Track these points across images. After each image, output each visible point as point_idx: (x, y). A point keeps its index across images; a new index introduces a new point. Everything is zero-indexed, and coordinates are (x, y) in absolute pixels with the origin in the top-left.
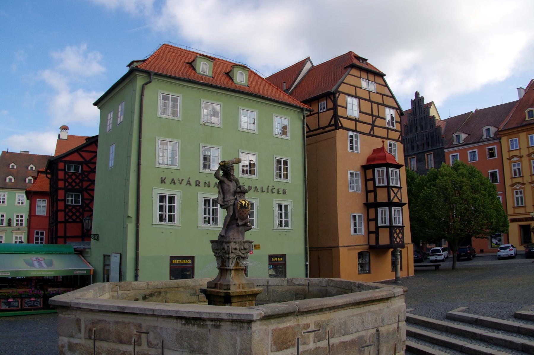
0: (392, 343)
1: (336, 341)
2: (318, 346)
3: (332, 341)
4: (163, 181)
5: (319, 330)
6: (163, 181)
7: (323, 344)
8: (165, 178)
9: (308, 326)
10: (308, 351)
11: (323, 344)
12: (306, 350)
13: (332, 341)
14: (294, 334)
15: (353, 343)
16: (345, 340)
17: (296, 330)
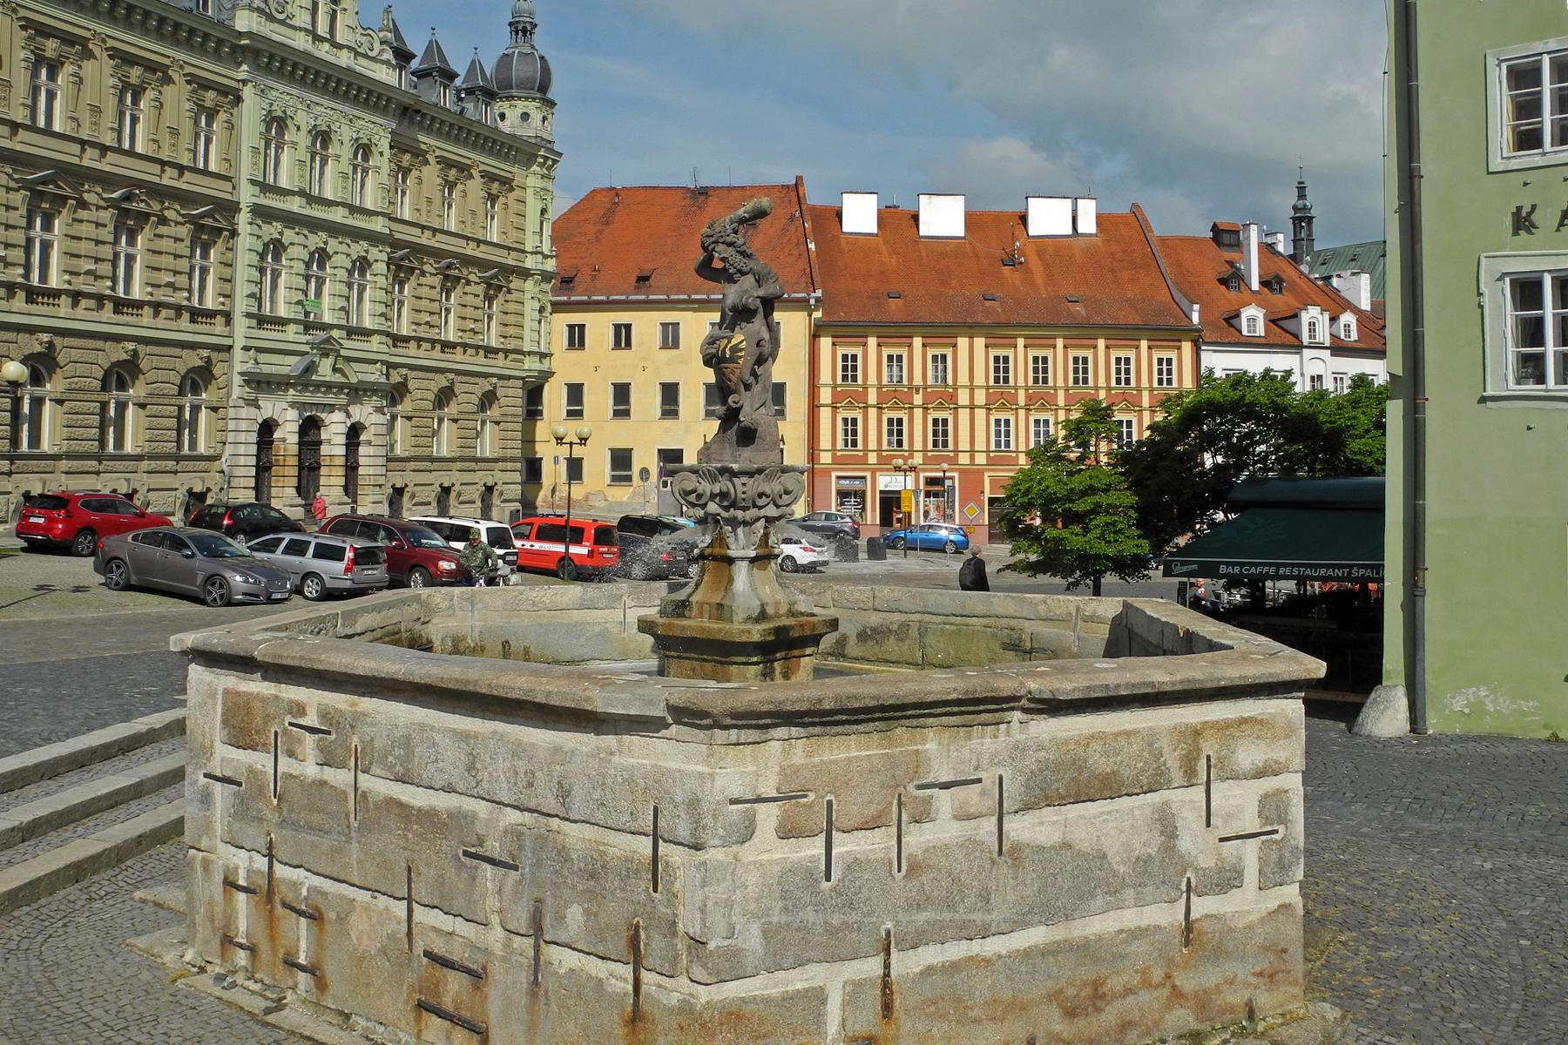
0: (615, 912)
1: (378, 786)
2: (325, 777)
3: (365, 781)
4: (1522, 222)
5: (328, 733)
6: (1522, 222)
7: (340, 778)
8: (1534, 207)
9: (301, 710)
10: (296, 777)
11: (340, 778)
12: (295, 773)
13: (365, 781)
14: (267, 719)
15: (428, 816)
16: (404, 799)
17: (271, 710)
